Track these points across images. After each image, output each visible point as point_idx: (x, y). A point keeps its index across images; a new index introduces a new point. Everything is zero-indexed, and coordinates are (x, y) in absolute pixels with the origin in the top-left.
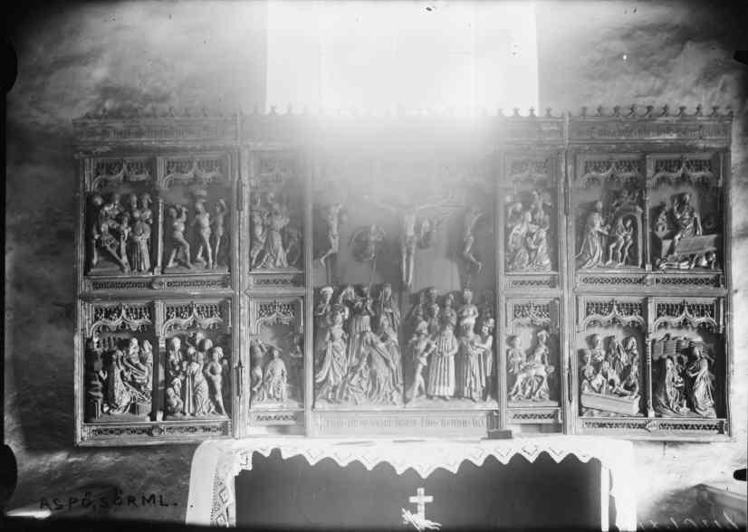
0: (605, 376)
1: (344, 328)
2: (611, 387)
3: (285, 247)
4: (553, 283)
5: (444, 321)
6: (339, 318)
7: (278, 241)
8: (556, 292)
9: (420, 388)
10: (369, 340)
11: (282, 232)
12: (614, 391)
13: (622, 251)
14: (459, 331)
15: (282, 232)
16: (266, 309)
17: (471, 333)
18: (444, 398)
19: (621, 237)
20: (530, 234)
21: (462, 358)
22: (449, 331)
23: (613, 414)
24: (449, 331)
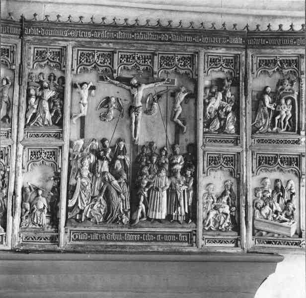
0: (272, 207)
1: (90, 169)
2: (275, 216)
3: (51, 111)
4: (236, 142)
5: (160, 166)
6: (87, 162)
7: (46, 105)
8: (237, 149)
9: (142, 212)
10: (107, 178)
11: (49, 101)
12: (277, 218)
13: (284, 121)
14: (171, 174)
15: (49, 101)
16: (35, 155)
17: (179, 175)
18: (160, 221)
19: (283, 113)
20: (221, 108)
21: (172, 192)
22: (163, 173)
23: (276, 235)
24: (163, 173)
